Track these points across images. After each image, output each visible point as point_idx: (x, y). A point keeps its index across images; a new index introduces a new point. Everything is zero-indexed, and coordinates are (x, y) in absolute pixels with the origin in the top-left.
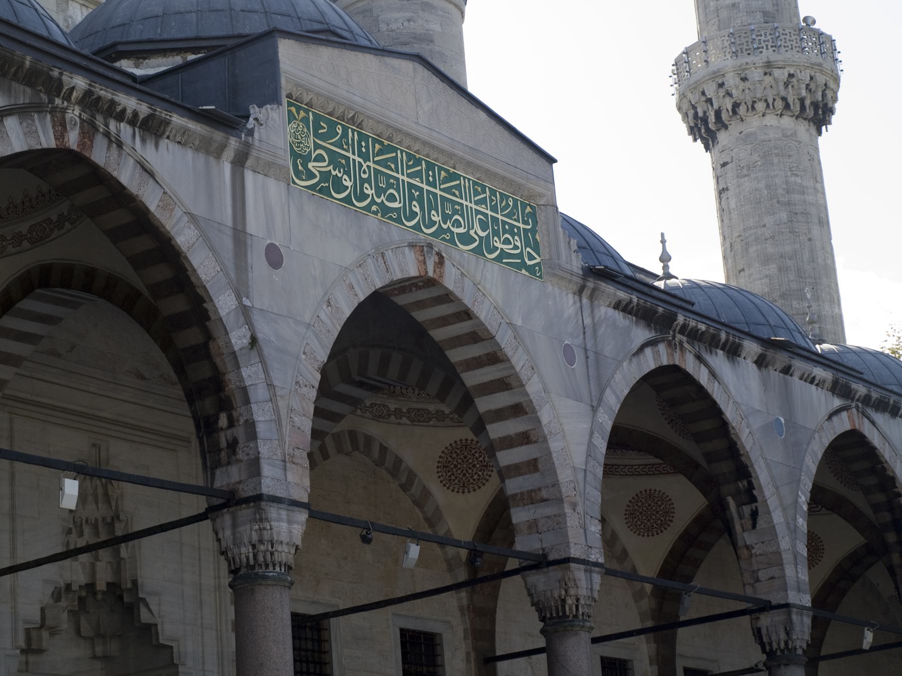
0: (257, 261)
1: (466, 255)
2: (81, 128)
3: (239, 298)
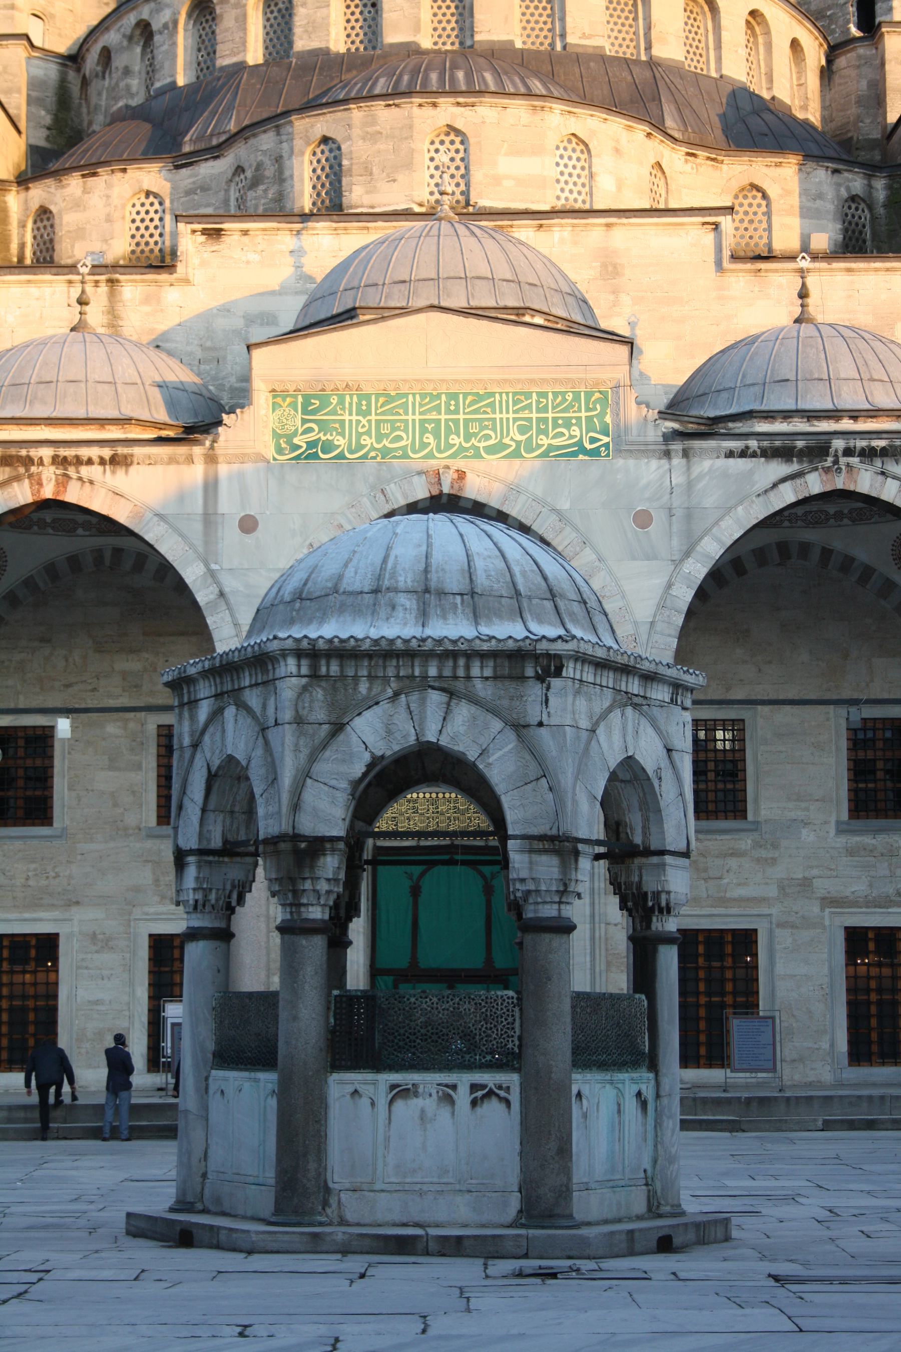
0: (230, 534)
1: (495, 463)
2: (57, 480)
3: (207, 565)
